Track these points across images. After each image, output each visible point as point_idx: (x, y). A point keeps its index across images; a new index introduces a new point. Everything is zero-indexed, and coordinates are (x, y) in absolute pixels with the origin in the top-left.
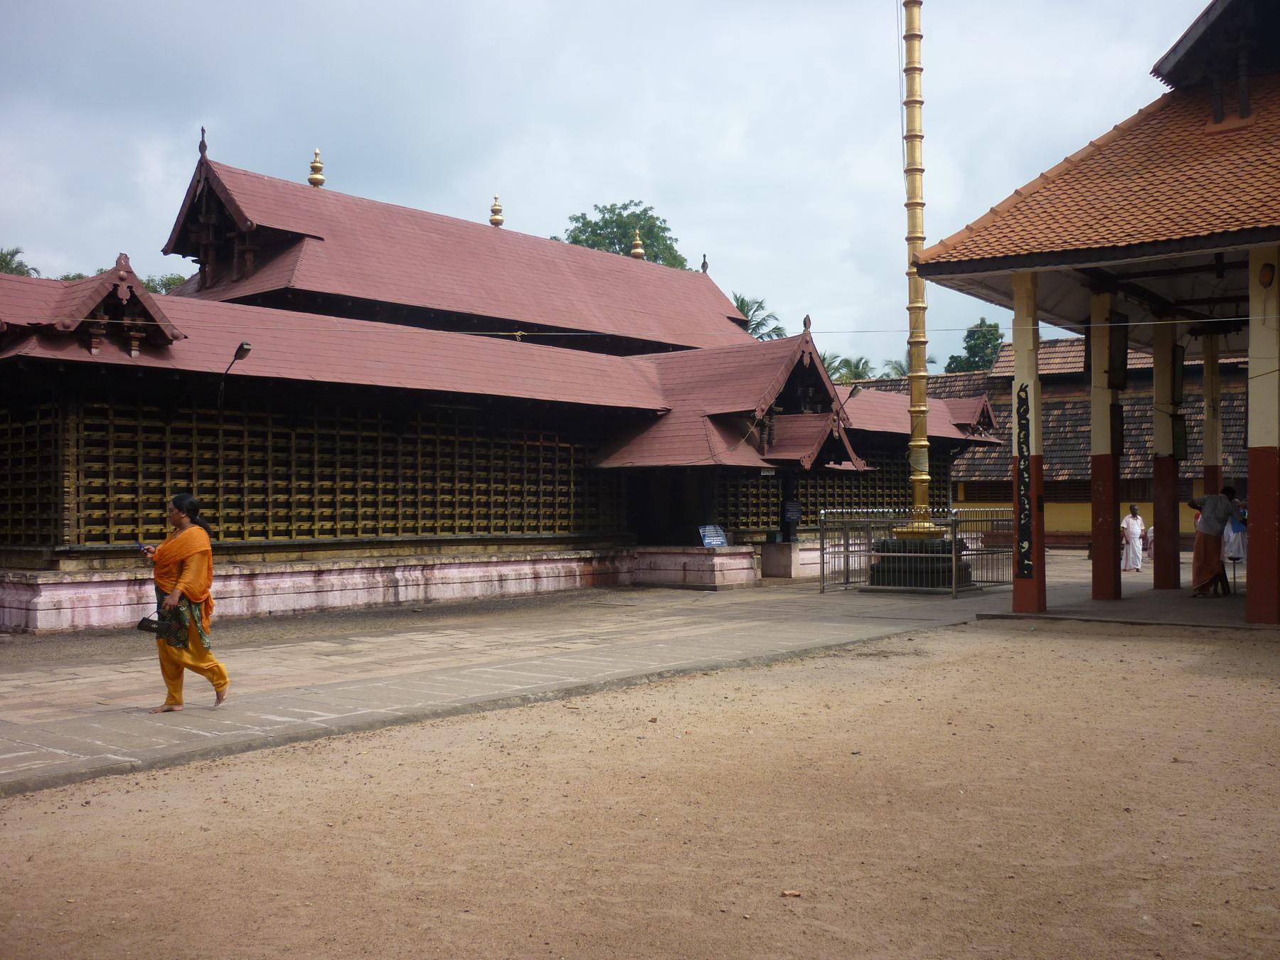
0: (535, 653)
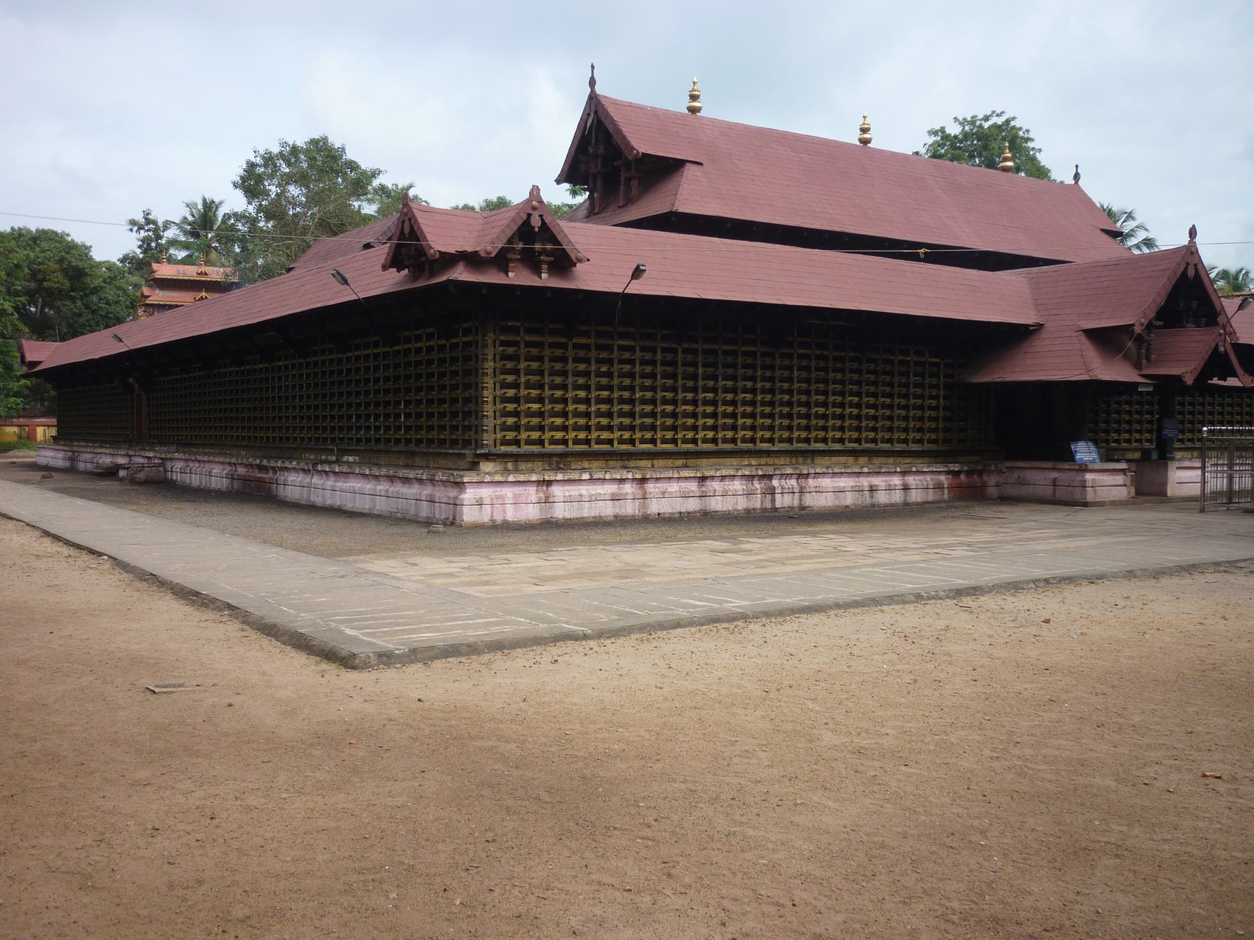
0: (917, 558)
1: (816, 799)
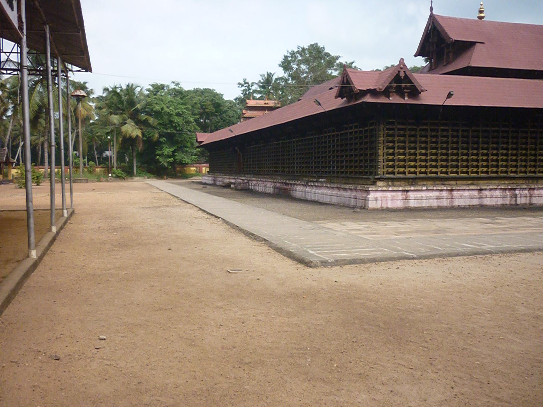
1: (510, 337)
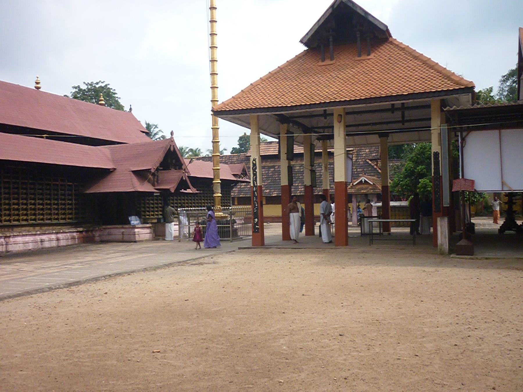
0: (56, 270)
